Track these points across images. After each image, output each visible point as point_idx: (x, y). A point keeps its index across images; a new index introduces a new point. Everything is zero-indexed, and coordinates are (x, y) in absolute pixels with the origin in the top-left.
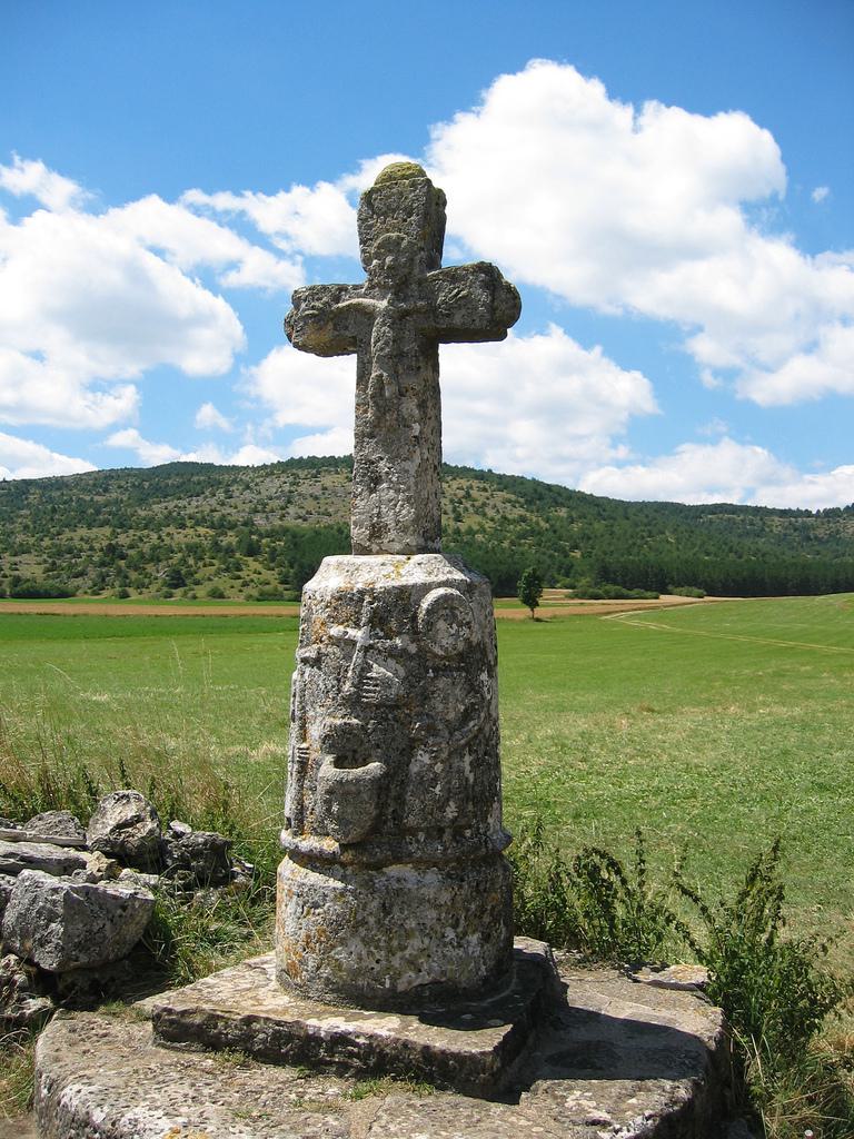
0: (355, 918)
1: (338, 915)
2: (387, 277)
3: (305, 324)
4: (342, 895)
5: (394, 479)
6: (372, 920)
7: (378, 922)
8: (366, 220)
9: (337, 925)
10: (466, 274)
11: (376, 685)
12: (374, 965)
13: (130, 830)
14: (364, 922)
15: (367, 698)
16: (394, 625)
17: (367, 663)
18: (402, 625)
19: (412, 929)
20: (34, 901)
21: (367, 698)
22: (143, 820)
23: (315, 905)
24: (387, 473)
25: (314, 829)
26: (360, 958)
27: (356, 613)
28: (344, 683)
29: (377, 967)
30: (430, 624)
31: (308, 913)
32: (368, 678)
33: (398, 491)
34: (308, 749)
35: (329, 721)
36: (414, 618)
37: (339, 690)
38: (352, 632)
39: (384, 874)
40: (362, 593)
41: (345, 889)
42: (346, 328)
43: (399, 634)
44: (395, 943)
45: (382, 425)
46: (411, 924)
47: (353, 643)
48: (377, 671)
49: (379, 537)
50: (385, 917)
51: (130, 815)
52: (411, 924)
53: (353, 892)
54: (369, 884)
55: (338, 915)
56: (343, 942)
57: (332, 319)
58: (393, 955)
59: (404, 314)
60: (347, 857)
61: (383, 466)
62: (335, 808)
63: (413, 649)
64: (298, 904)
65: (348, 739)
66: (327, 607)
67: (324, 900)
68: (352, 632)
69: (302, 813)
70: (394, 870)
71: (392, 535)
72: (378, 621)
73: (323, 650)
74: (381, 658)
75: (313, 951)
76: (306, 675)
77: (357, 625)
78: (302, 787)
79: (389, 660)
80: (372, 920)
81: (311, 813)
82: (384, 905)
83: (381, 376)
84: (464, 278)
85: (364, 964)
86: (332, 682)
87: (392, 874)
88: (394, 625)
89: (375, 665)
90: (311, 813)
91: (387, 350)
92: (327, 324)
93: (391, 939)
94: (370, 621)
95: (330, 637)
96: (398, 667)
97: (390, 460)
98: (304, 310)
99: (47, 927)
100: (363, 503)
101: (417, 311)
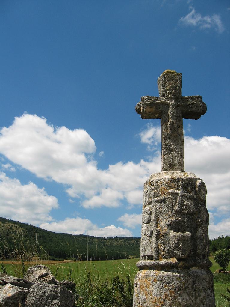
0: (184, 286)
1: (178, 285)
2: (173, 96)
3: (146, 106)
4: (179, 278)
5: (177, 150)
6: (190, 286)
7: (192, 287)
8: (164, 81)
9: (178, 289)
10: (195, 98)
11: (187, 207)
12: (191, 303)
13: (44, 278)
14: (187, 287)
15: (184, 211)
16: (189, 189)
17: (183, 200)
18: (192, 189)
19: (201, 289)
20: (45, 292)
21: (184, 211)
22: (48, 275)
23: (169, 283)
24: (174, 149)
25: (164, 257)
26: (187, 301)
27: (177, 185)
28: (175, 207)
29: (192, 304)
30: (200, 189)
31: (165, 286)
32: (183, 205)
33: (179, 154)
34: (160, 230)
35: (170, 219)
36: (195, 188)
37: (173, 209)
38: (177, 191)
39: (191, 270)
40: (179, 179)
41: (180, 276)
42: (160, 108)
43: (191, 192)
44: (197, 294)
45: (173, 135)
46: (201, 287)
47: (177, 194)
48: (186, 203)
49: (173, 167)
50: (194, 285)
51: (44, 273)
52: (201, 287)
53: (183, 277)
54: (187, 273)
55: (178, 285)
56: (180, 295)
57: (155, 105)
58: (197, 299)
59: (178, 106)
60: (181, 264)
61: (173, 147)
62: (181, 245)
63: (195, 197)
64: (160, 284)
65: (178, 225)
66: (166, 184)
67: (173, 280)
68: (177, 191)
69: (158, 252)
70: (194, 269)
71: (177, 166)
72: (185, 188)
73: (166, 197)
74: (187, 199)
75: (168, 300)
76: (157, 206)
77: (178, 189)
78: (158, 243)
79: (189, 200)
80: (190, 286)
81: (163, 251)
82: (193, 281)
83: (173, 121)
84: (194, 99)
85: (188, 302)
86: (170, 207)
87: (193, 270)
88: (189, 189)
89: (185, 201)
90: (163, 251)
91: (175, 114)
92: (153, 106)
93: (196, 293)
94: (182, 188)
95: (169, 193)
96: (192, 202)
97: (175, 145)
98: (146, 102)
99: (52, 302)
100: (167, 157)
101: (182, 106)
